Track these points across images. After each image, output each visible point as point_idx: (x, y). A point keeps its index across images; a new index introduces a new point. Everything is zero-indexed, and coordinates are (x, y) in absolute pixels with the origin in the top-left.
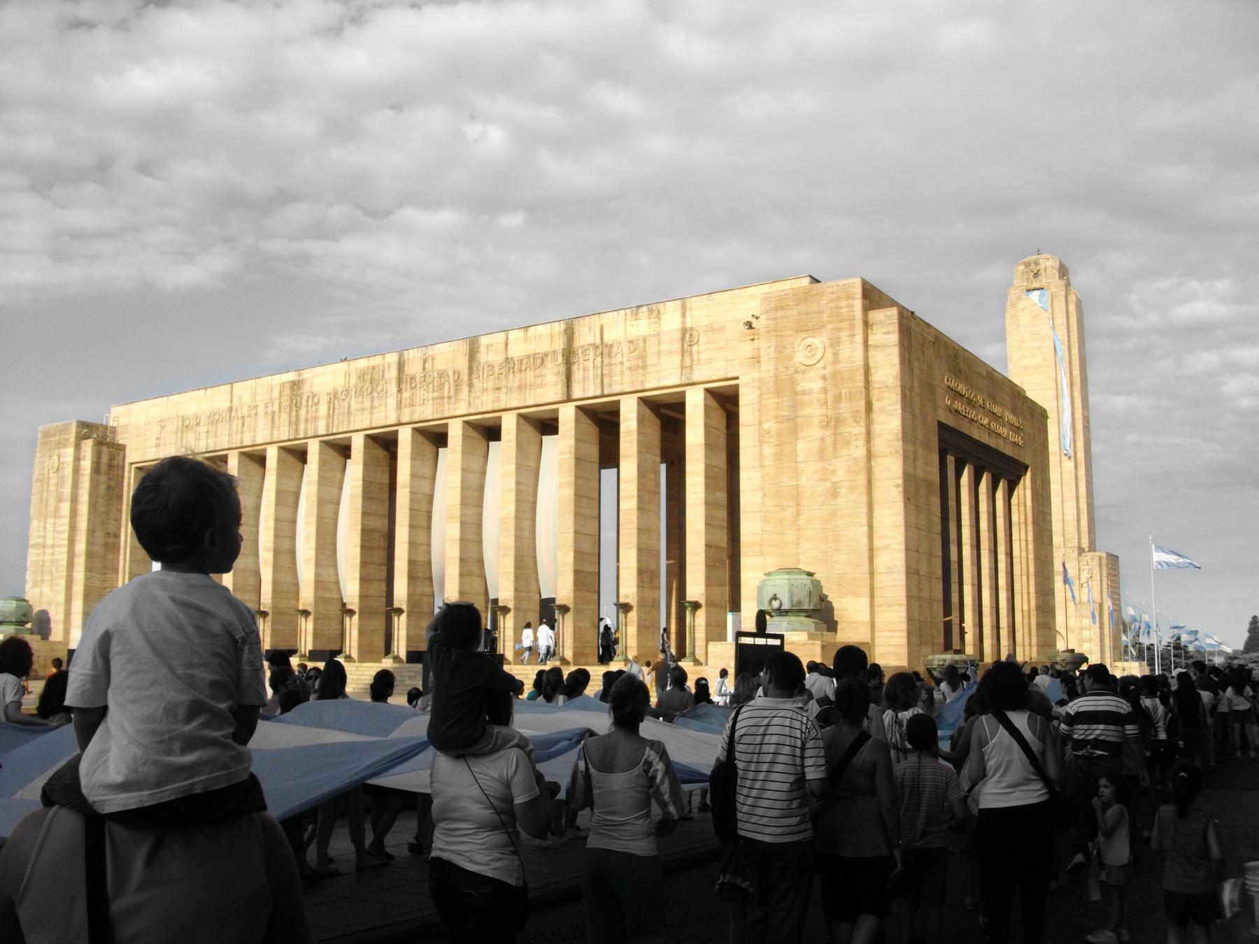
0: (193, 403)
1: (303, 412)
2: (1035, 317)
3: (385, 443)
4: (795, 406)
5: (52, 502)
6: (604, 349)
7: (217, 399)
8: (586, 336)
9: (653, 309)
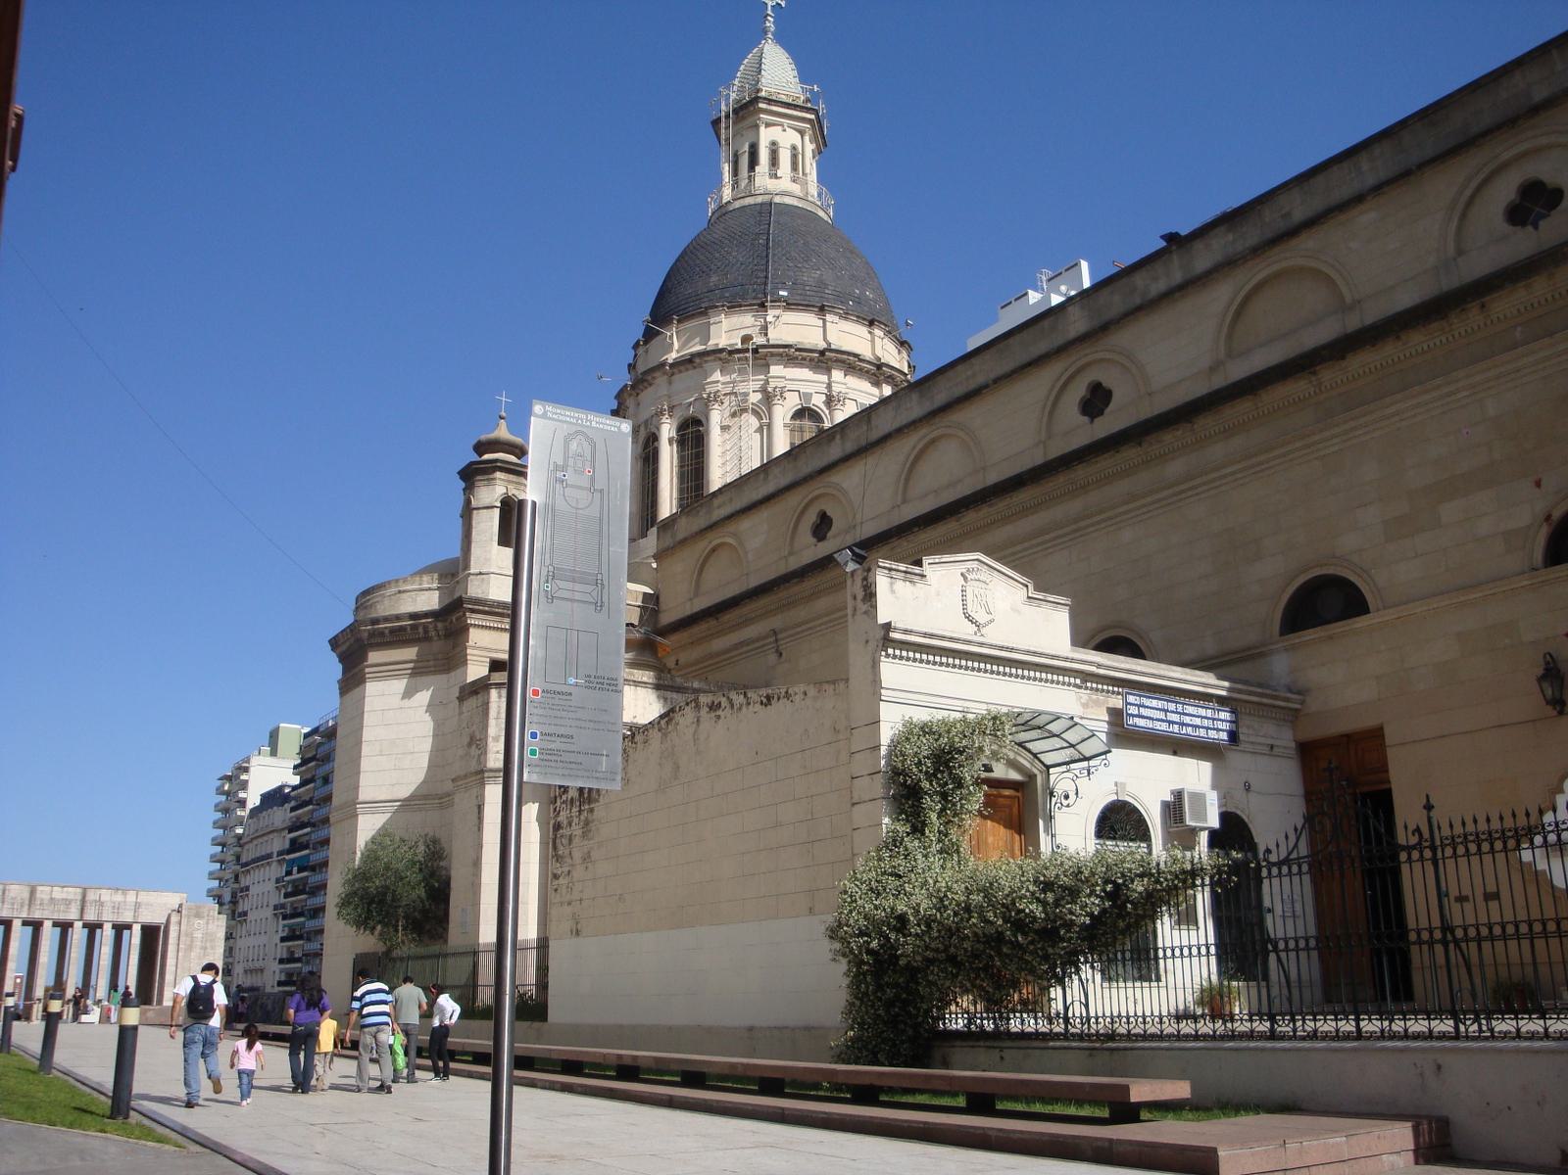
4: (192, 941)
6: (102, 904)
8: (91, 896)
9: (125, 891)
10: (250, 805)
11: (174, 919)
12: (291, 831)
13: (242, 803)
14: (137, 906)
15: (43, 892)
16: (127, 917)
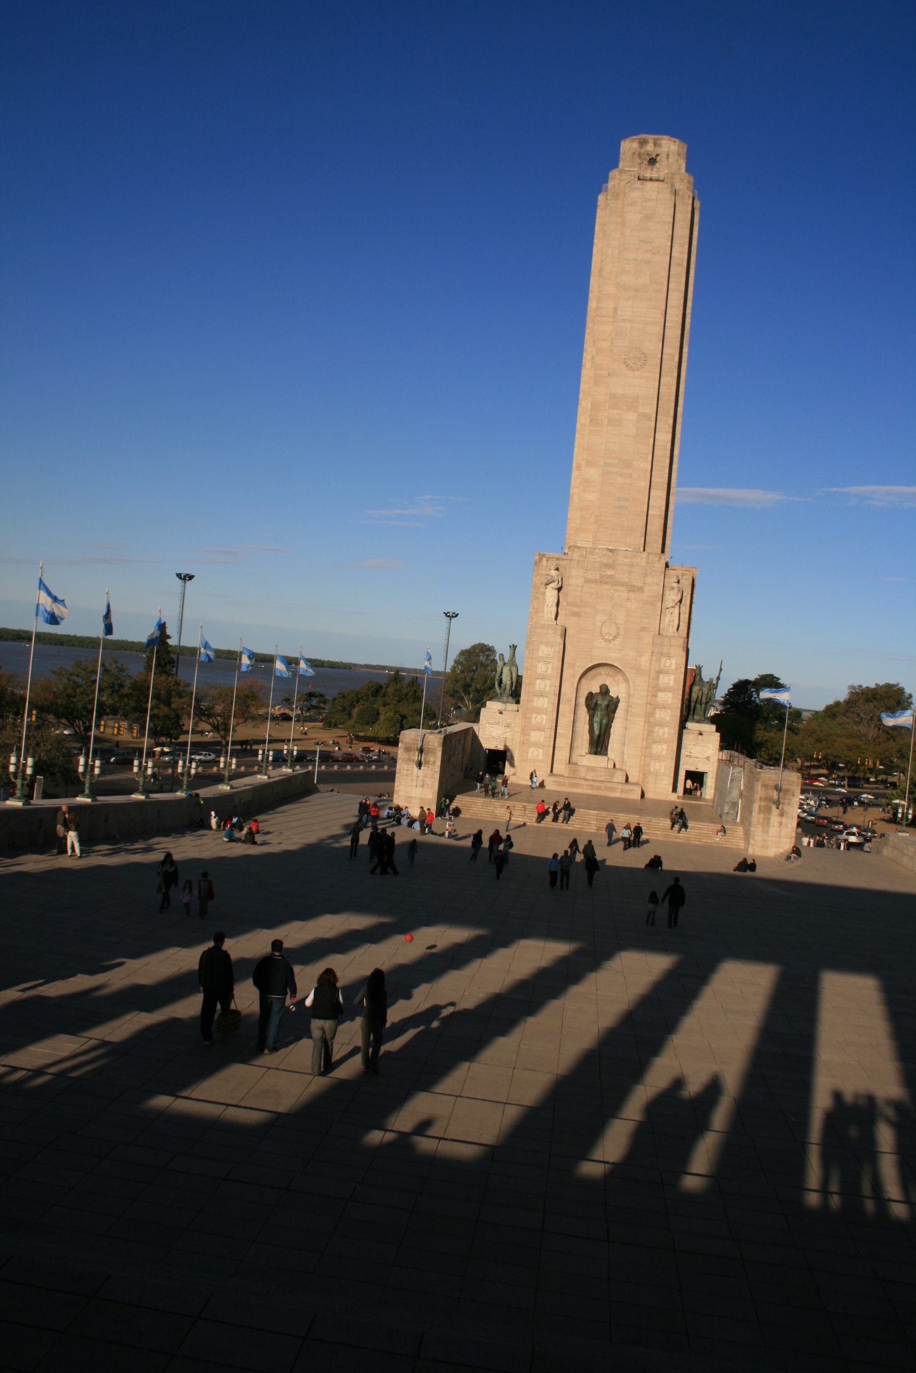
2: (649, 218)
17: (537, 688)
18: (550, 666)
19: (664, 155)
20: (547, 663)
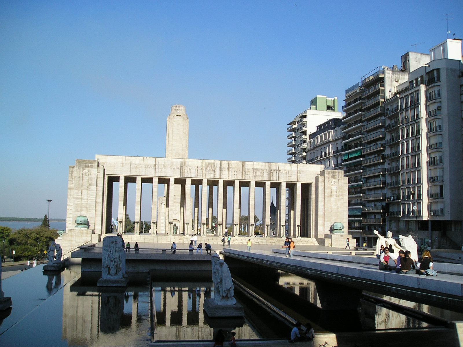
0: (137, 160)
1: (186, 171)
3: (213, 183)
4: (331, 192)
5: (85, 185)
7: (150, 161)
10: (309, 133)
11: (320, 179)
12: (344, 138)
13: (304, 133)
14: (298, 172)
15: (249, 165)
16: (293, 180)
17: (161, 225)
18: (164, 221)
19: (181, 110)
20: (163, 220)
